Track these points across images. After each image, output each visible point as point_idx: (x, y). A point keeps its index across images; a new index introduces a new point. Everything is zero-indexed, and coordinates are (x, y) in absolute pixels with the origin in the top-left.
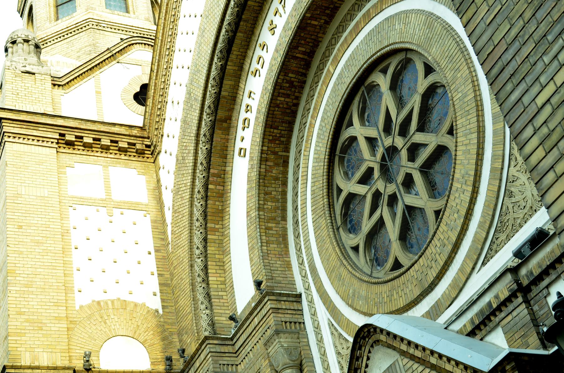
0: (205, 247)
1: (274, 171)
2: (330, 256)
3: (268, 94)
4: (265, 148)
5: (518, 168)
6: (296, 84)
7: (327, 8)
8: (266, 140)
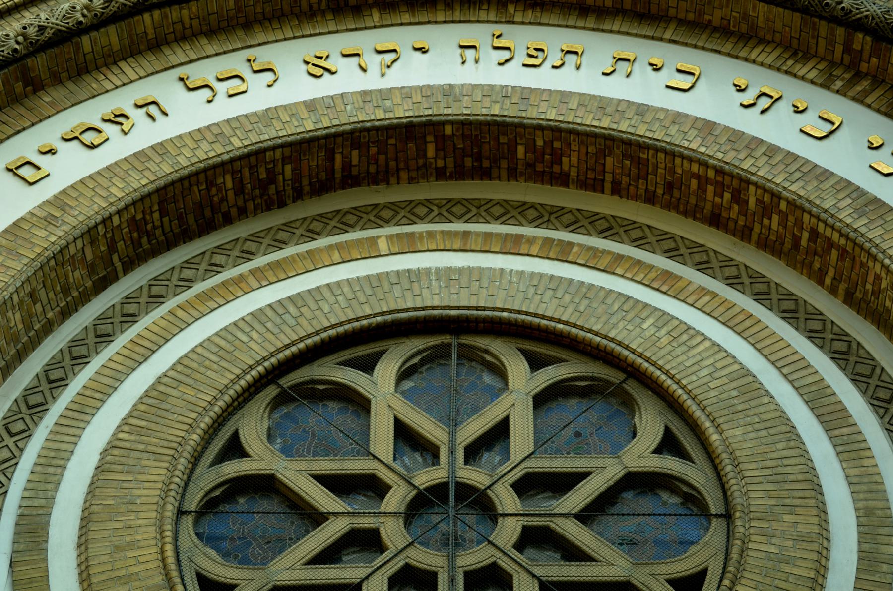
1: (77, 274)
2: (132, 545)
4: (116, 220)
6: (272, 190)
7: (479, 157)
8: (133, 211)
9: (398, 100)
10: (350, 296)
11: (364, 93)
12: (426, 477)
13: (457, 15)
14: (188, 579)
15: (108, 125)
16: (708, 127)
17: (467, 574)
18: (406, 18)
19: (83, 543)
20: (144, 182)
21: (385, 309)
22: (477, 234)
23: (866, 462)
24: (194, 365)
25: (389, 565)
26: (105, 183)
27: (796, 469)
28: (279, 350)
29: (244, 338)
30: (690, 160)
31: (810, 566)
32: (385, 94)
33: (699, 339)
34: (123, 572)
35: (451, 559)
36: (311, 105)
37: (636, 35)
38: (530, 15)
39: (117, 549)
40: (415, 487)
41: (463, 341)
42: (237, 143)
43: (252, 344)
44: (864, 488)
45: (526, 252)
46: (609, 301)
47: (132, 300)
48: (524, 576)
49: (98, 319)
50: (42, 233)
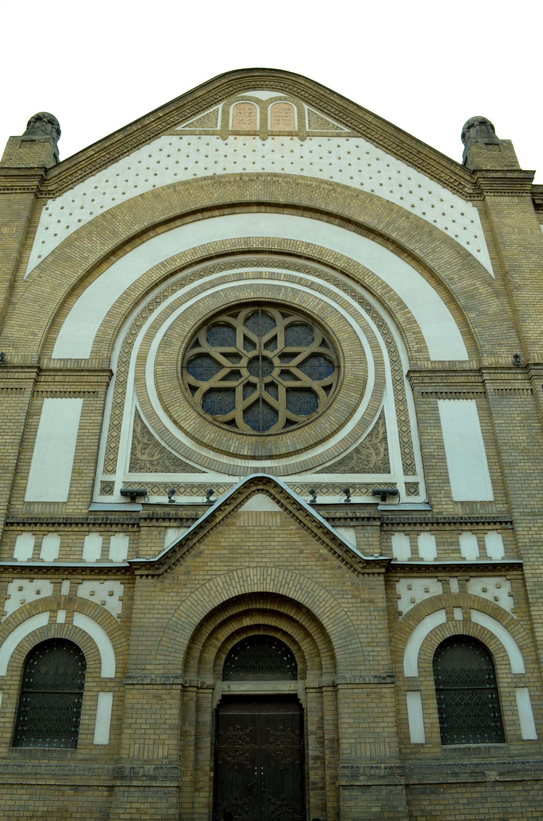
5: (371, 443)
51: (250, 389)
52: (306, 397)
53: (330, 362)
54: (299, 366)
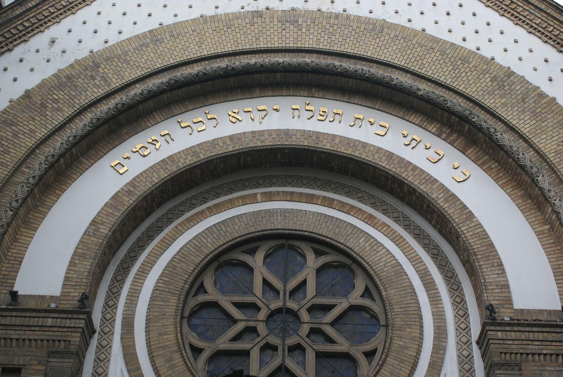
0: (21, 206)
1: (140, 213)
2: (166, 333)
3: (195, 160)
4: (155, 192)
9: (266, 137)
10: (246, 222)
11: (253, 132)
12: (275, 305)
13: (291, 92)
14: (186, 346)
15: (150, 144)
16: (390, 155)
17: (289, 347)
18: (270, 93)
19: (148, 331)
20: (166, 175)
21: (260, 230)
22: (297, 193)
23: (440, 306)
24: (186, 253)
25: (260, 343)
26: (150, 175)
27: (413, 309)
28: (219, 247)
29: (205, 241)
30: (382, 171)
31: (415, 351)
32: (261, 133)
33: (381, 248)
34: (162, 345)
35: (284, 341)
36: (231, 137)
37: (364, 106)
38: (321, 94)
39: (160, 334)
40: (270, 309)
41: (291, 243)
42: (202, 157)
43: (208, 244)
44: (438, 317)
45: (316, 203)
46: (347, 229)
47: (160, 220)
48: (310, 349)
49: (147, 228)
50: (127, 199)
51: (270, 352)
52: (341, 365)
53: (374, 317)
54: (333, 324)
